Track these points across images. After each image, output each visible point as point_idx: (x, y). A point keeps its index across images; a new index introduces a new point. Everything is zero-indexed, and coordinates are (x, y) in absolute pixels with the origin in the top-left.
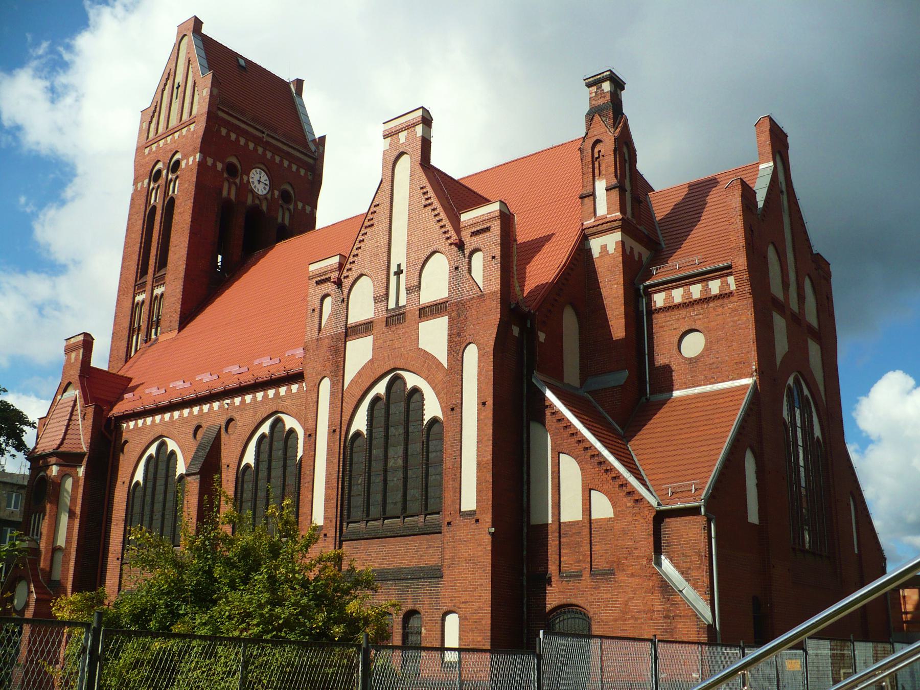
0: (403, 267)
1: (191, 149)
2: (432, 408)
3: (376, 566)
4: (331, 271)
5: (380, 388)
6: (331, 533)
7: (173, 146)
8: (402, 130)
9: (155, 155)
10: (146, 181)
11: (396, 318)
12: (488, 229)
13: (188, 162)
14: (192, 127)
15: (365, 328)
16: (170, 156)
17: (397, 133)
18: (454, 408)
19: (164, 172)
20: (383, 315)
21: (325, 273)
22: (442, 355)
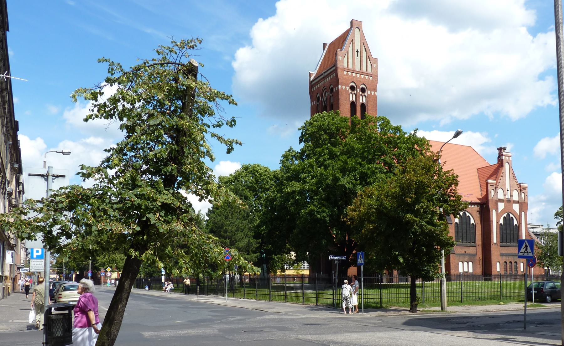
0: (509, 190)
1: (372, 88)
2: (515, 222)
3: (507, 252)
4: (494, 184)
5: (505, 215)
6: (499, 245)
7: (361, 80)
8: (507, 156)
9: (351, 78)
10: (348, 88)
11: (509, 201)
12: (525, 189)
13: (371, 93)
14: (371, 78)
15: (502, 201)
16: (361, 84)
17: (506, 156)
18: (520, 223)
19: (358, 90)
20: (506, 199)
21: (492, 184)
22: (518, 212)
